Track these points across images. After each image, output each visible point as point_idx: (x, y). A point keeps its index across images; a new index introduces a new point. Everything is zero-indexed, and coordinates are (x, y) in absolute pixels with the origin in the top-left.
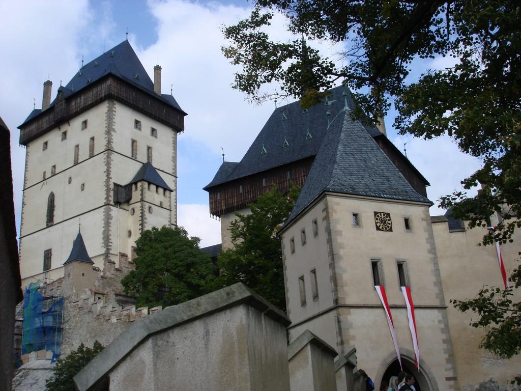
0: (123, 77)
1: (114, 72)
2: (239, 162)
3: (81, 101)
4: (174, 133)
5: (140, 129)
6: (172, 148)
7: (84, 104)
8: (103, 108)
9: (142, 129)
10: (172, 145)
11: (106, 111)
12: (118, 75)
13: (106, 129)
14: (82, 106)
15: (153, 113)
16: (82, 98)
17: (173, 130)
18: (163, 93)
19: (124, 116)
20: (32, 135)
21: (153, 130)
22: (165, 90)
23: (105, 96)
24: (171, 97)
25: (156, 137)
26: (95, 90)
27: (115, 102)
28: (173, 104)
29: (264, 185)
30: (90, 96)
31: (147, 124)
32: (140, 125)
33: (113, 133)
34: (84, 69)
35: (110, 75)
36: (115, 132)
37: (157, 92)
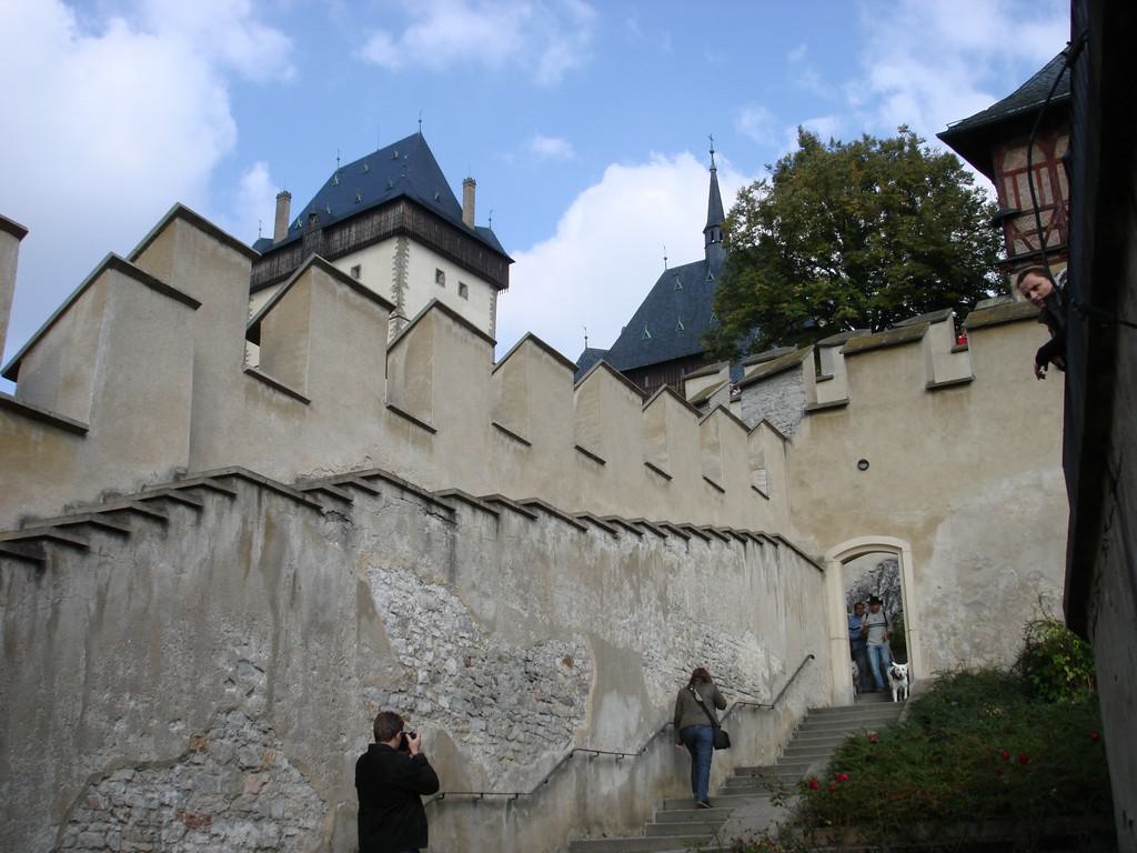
0: (421, 199)
1: (408, 192)
2: (608, 349)
3: (352, 234)
4: (492, 291)
5: (443, 285)
6: (488, 316)
7: (357, 238)
8: (389, 249)
9: (446, 285)
10: (489, 311)
11: (395, 254)
12: (414, 197)
13: (394, 283)
14: (352, 243)
15: (464, 259)
16: (353, 229)
17: (491, 287)
18: (476, 224)
19: (421, 263)
20: (260, 282)
21: (462, 286)
22: (480, 221)
23: (394, 230)
24: (488, 231)
25: (466, 298)
26: (376, 219)
27: (408, 240)
28: (493, 245)
29: (647, 385)
30: (368, 228)
31: (454, 276)
32: (444, 278)
33: (404, 289)
34: (340, 172)
35: (403, 198)
36: (408, 288)
37: (468, 224)
